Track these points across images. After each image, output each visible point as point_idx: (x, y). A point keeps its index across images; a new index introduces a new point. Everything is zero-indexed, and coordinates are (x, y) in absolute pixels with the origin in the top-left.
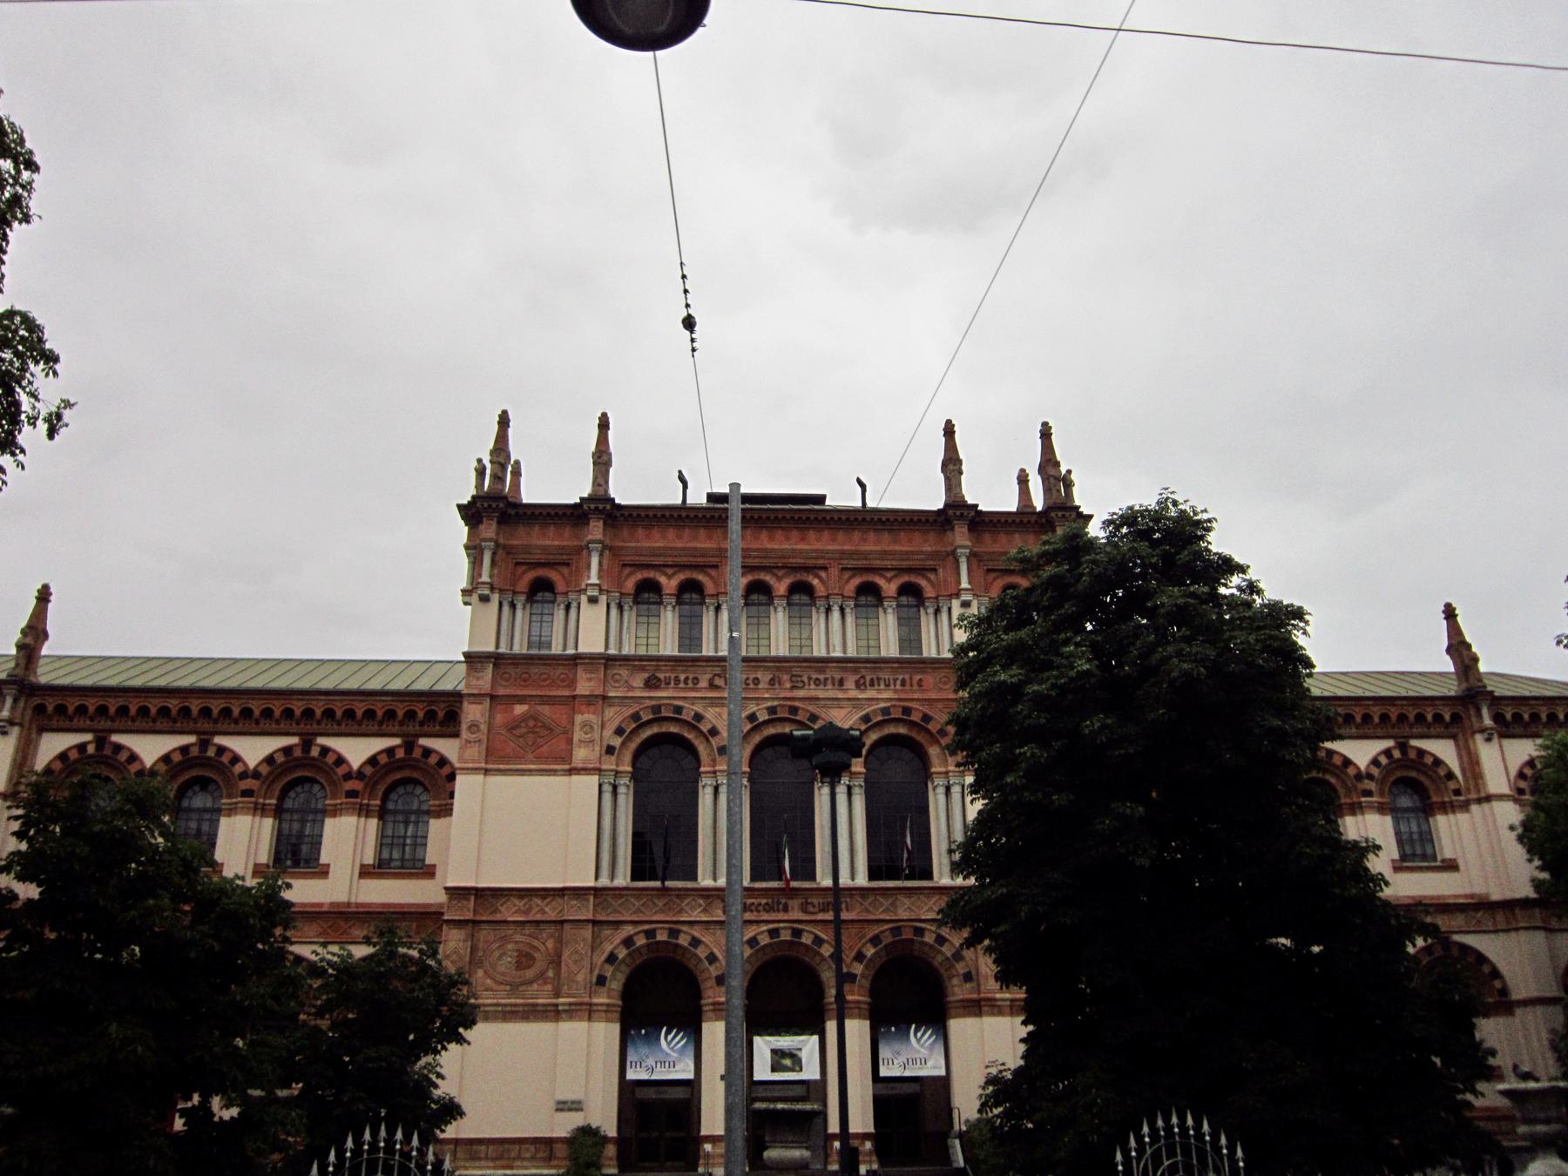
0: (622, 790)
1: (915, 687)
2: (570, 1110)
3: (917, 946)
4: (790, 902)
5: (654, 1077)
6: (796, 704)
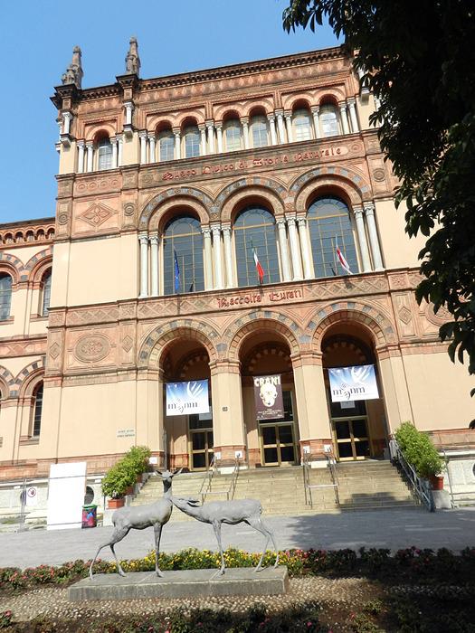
1: (335, 154)
5: (184, 413)
6: (258, 175)
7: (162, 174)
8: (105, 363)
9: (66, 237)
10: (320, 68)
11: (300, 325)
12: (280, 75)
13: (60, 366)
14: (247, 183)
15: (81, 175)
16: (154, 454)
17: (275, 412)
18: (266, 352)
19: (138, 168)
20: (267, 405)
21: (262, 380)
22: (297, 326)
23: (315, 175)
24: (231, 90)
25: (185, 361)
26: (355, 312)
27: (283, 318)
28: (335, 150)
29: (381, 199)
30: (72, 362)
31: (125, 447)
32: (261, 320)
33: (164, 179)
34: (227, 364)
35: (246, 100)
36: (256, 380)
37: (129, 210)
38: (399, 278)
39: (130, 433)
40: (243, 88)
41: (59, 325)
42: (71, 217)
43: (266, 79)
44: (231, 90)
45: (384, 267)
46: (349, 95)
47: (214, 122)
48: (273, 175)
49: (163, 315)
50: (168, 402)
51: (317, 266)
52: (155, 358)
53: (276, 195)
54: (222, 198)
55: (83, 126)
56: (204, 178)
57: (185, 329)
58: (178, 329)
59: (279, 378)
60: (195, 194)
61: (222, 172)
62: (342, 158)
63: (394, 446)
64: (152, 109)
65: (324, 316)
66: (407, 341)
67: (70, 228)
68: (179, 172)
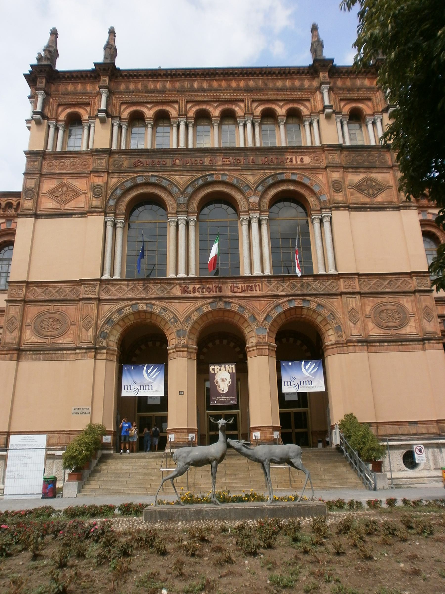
0: (119, 225)
1: (299, 162)
2: (82, 413)
3: (305, 312)
4: (223, 286)
6: (226, 173)
7: (133, 161)
8: (66, 339)
9: (31, 212)
10: (288, 83)
11: (258, 317)
12: (251, 83)
13: (17, 340)
14: (214, 178)
15: (50, 153)
16: (105, 433)
17: (228, 398)
18: (217, 342)
19: (109, 152)
20: (221, 392)
21: (217, 367)
22: (255, 319)
23: (279, 179)
24: (204, 91)
25: (141, 345)
26: (309, 309)
27: (242, 309)
28: (299, 158)
29: (337, 208)
30: (30, 337)
31: (81, 423)
32: (220, 309)
33: (135, 166)
34: (186, 349)
35: (219, 101)
36: (212, 367)
37: (97, 191)
38: (350, 282)
39: (85, 411)
40: (216, 90)
41: (18, 299)
42: (38, 194)
43: (238, 85)
44: (204, 91)
45: (336, 270)
46: (314, 111)
47: (187, 117)
48: (240, 174)
49: (125, 297)
50: (125, 382)
51: (275, 264)
52: (113, 341)
53: (241, 192)
54: (190, 190)
55: (55, 106)
56: (174, 169)
57: (145, 312)
58: (139, 312)
59: (234, 366)
60: (164, 183)
61: (191, 166)
62: (304, 167)
63: (336, 438)
64: (127, 98)
65: (280, 310)
66: (354, 340)
67: (37, 204)
68: (150, 160)
